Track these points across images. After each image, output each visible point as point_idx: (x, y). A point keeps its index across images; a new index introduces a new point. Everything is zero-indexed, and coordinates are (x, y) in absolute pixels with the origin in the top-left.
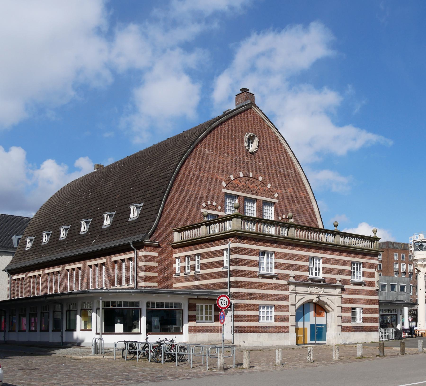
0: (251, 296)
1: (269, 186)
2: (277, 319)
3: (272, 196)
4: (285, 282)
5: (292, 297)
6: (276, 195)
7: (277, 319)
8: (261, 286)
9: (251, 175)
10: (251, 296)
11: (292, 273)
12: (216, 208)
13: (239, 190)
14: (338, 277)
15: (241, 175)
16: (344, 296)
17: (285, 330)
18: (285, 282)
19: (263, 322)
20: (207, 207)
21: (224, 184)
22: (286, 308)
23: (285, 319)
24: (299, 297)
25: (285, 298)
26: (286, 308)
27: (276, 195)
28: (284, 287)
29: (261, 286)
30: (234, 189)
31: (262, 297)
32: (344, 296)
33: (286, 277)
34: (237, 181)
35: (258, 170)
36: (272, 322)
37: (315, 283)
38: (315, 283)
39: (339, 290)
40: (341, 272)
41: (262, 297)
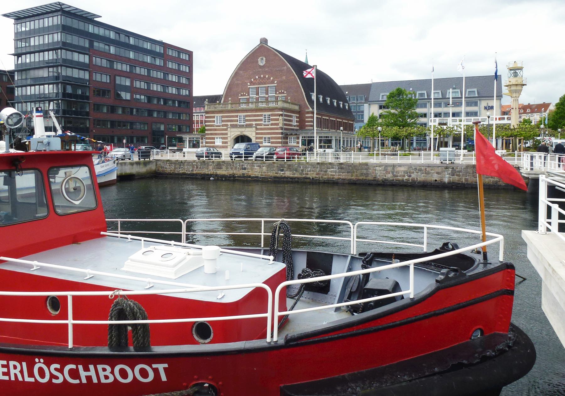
0: (211, 134)
1: (272, 78)
2: (223, 143)
3: (274, 83)
4: (225, 127)
5: (229, 134)
6: (276, 82)
7: (223, 143)
8: (215, 130)
9: (262, 76)
10: (211, 134)
11: (229, 123)
12: (245, 95)
13: (257, 84)
14: (254, 123)
15: (257, 77)
16: (257, 131)
17: (226, 147)
18: (225, 127)
19: (217, 144)
20: (242, 96)
21: (249, 84)
22: (227, 138)
23: (226, 143)
24: (232, 133)
25: (226, 134)
26: (227, 138)
27: (276, 82)
28: (226, 130)
29: (215, 130)
30: (254, 85)
31: (216, 134)
32: (257, 131)
33: (227, 125)
34: (255, 81)
35: (266, 73)
36: (221, 144)
37: (242, 126)
38: (242, 126)
39: (254, 129)
40: (256, 120)
41: (216, 134)
